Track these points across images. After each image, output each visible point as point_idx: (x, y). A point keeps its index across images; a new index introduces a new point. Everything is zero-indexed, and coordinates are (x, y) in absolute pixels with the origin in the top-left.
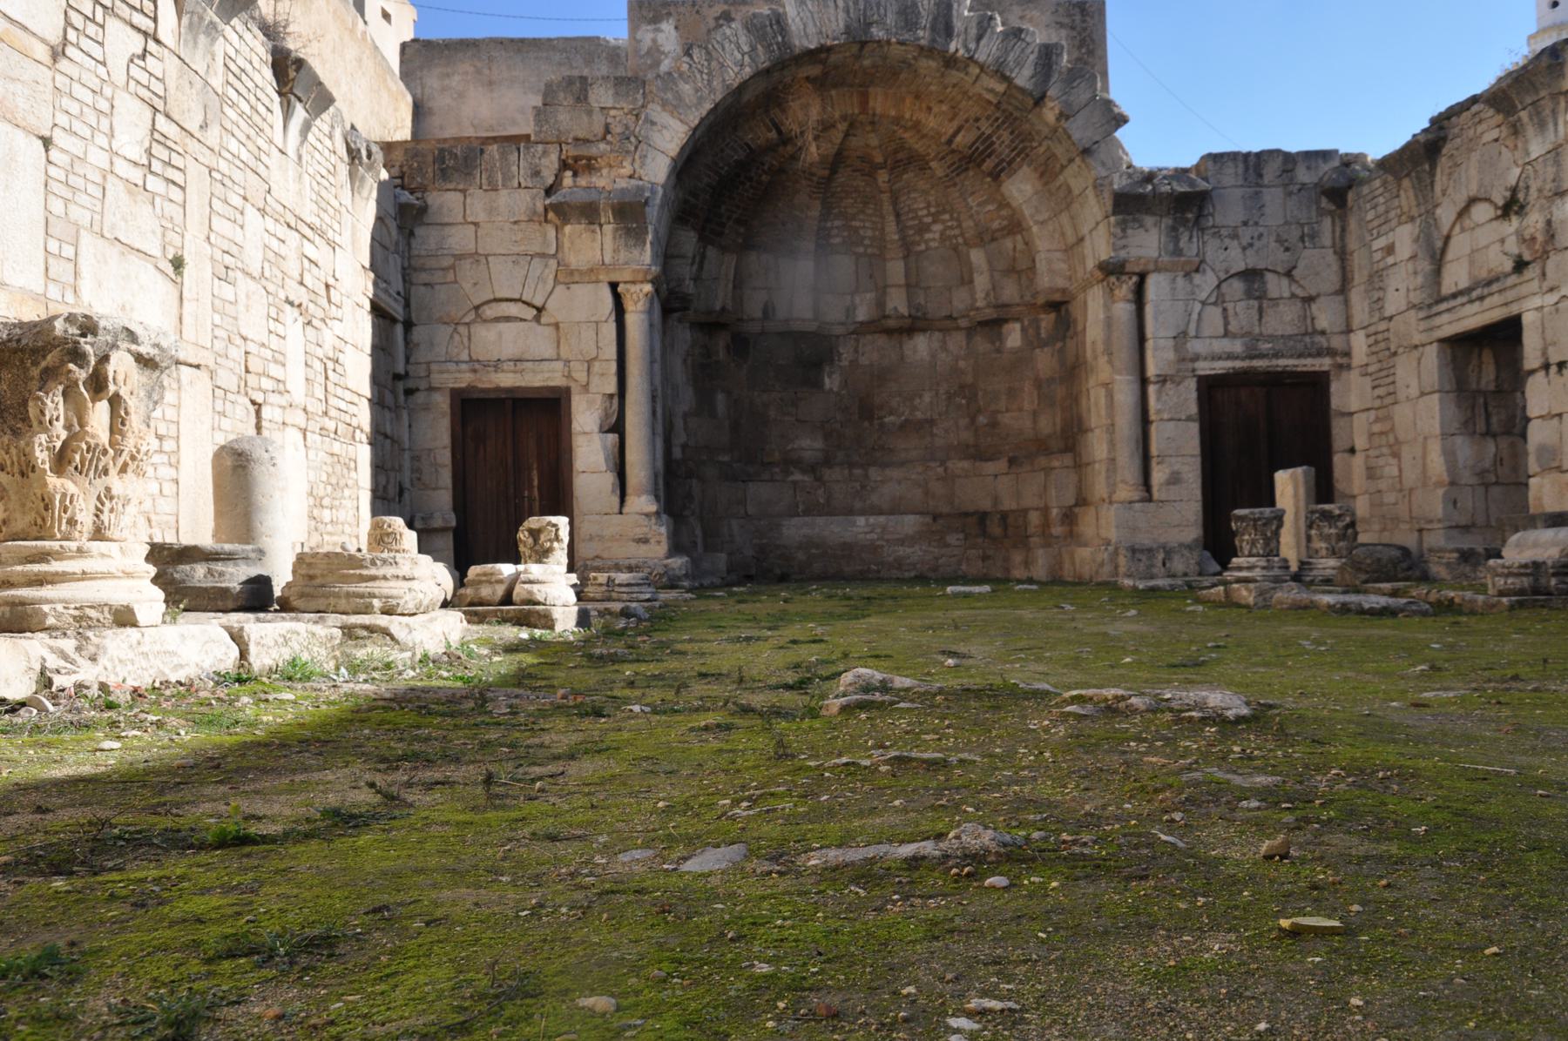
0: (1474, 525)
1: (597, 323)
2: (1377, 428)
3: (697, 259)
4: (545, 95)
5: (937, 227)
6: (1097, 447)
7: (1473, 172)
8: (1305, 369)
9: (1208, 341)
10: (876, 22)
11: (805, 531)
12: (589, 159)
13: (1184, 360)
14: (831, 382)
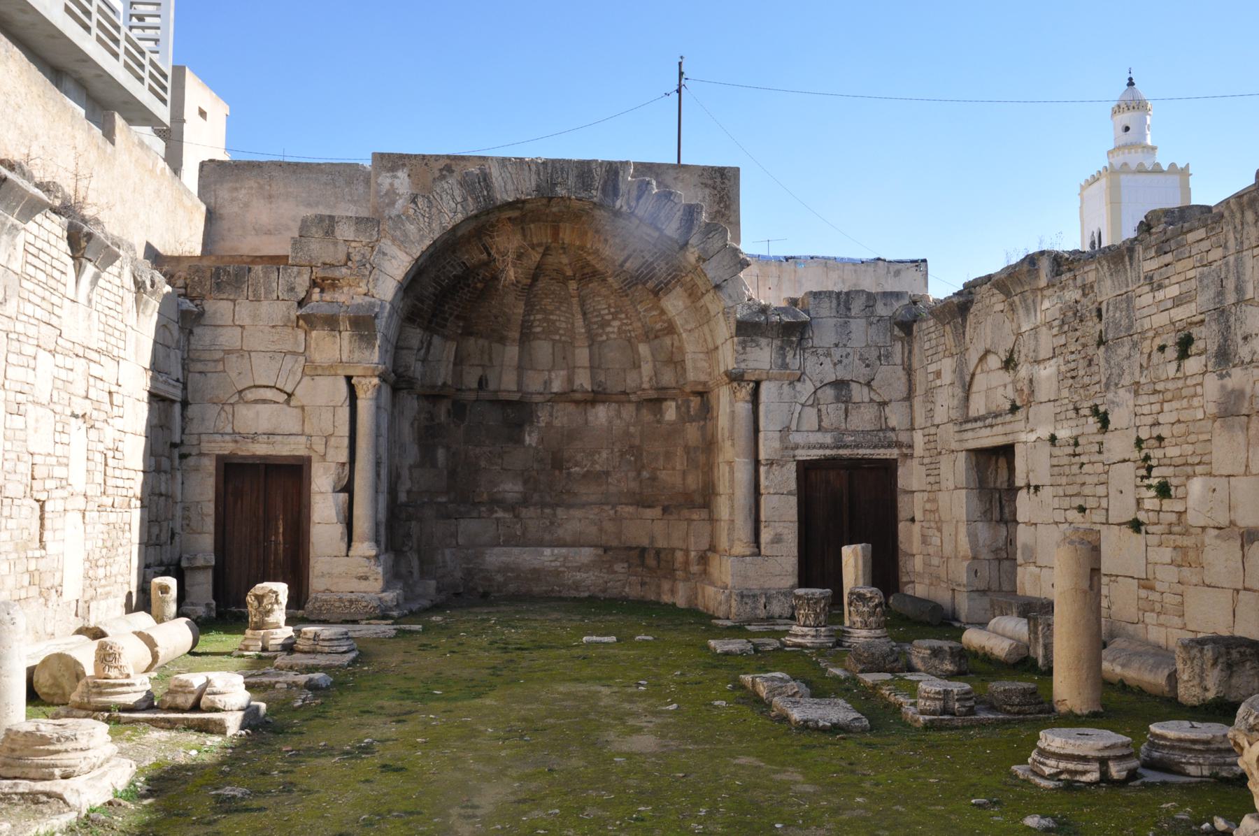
0: (989, 589)
1: (334, 407)
2: (928, 506)
3: (425, 345)
4: (301, 229)
5: (616, 323)
6: (723, 509)
7: (988, 331)
8: (878, 457)
11: (504, 558)
12: (333, 280)
13: (786, 448)
14: (531, 439)
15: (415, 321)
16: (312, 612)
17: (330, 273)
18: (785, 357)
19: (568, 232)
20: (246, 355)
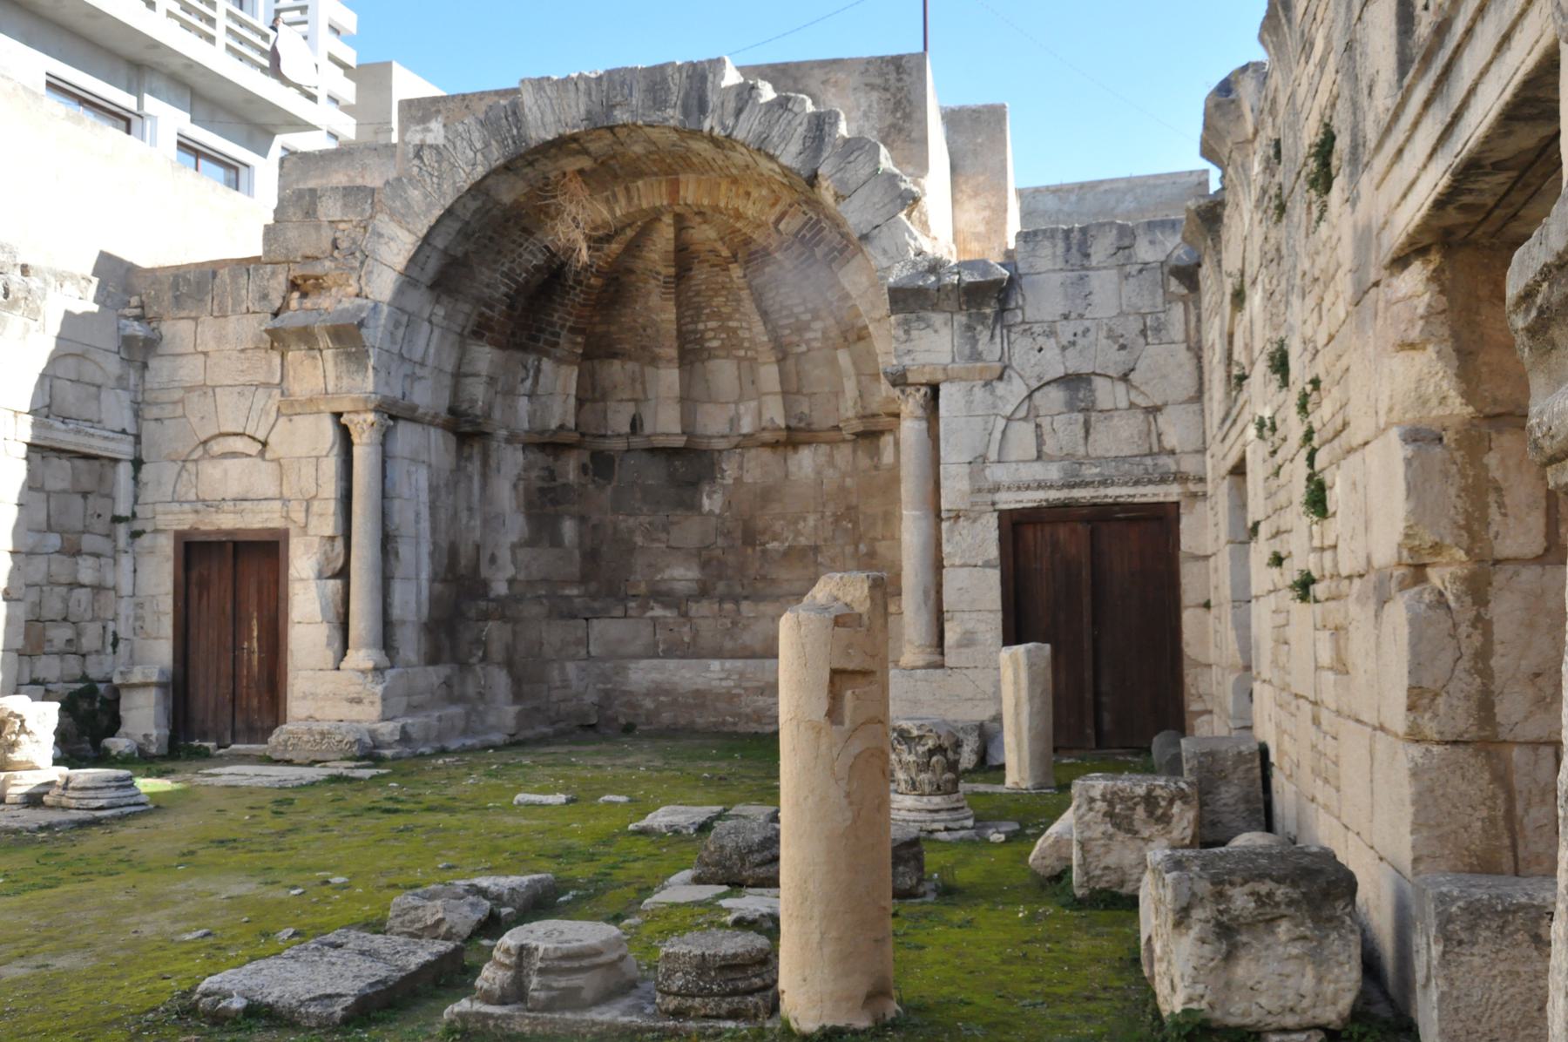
1: (317, 458)
3: (531, 373)
5: (818, 325)
9: (1014, 465)
10: (619, 104)
11: (656, 676)
12: (317, 278)
13: (980, 490)
14: (711, 502)
15: (483, 335)
16: (275, 749)
17: (309, 270)
18: (977, 341)
19: (691, 187)
20: (210, 393)
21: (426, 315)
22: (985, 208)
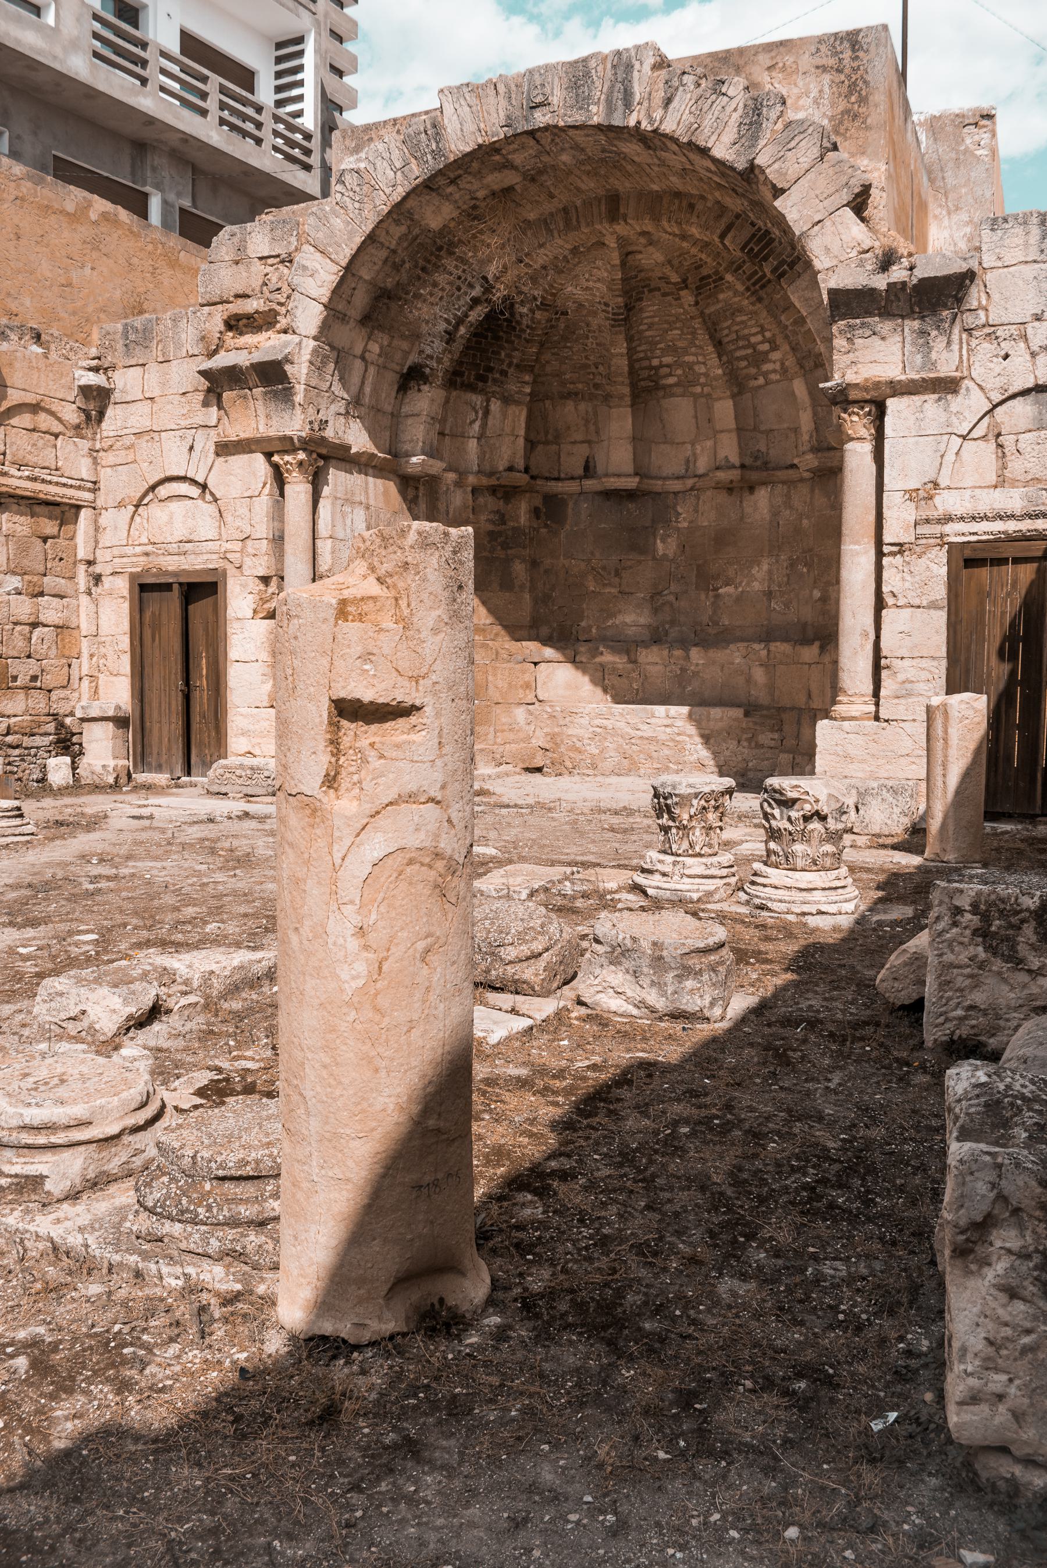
3: (480, 415)
5: (775, 356)
9: (969, 492)
14: (665, 547)
21: (358, 351)
22: (968, 223)
